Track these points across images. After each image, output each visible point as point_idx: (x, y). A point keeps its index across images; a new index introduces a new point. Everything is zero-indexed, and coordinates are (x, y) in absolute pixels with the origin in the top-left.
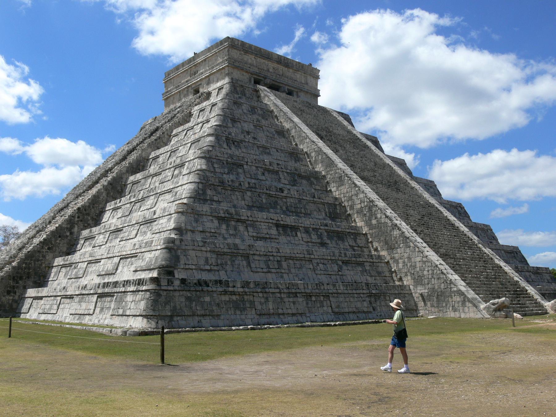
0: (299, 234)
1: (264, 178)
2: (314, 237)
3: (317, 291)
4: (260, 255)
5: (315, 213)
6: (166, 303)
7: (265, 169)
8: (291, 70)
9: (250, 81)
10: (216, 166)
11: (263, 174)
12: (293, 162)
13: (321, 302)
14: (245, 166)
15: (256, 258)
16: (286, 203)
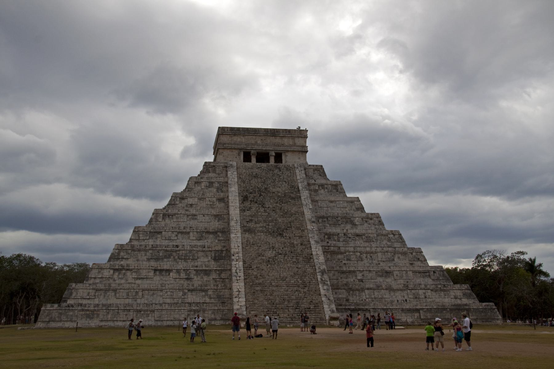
0: (171, 274)
1: (176, 238)
2: (183, 275)
3: (146, 308)
4: (124, 289)
5: (202, 258)
6: (47, 316)
7: (179, 233)
8: (278, 138)
10: (141, 236)
11: (177, 236)
12: (216, 221)
13: (148, 314)
14: (163, 233)
15: (122, 291)
16: (179, 254)
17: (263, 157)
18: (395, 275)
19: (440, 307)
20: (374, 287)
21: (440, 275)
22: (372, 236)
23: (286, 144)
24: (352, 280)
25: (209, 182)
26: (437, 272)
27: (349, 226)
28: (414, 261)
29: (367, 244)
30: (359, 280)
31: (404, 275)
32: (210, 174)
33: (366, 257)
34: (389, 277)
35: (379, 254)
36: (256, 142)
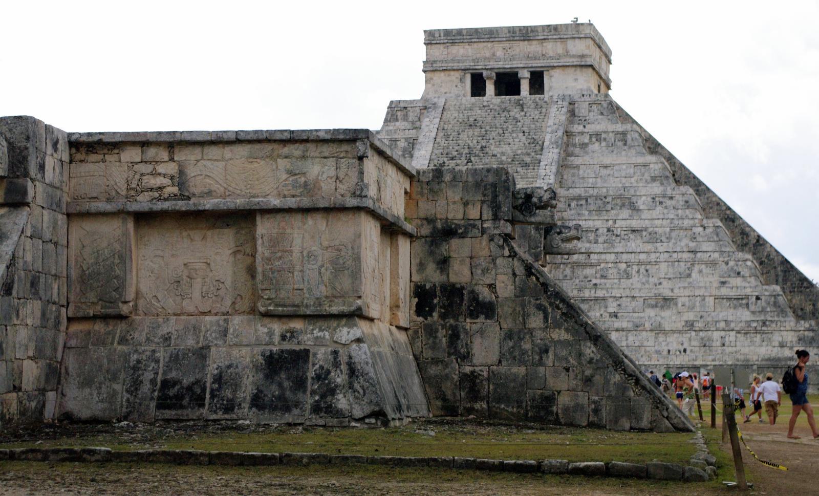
8: (534, 42)
9: (462, 80)
17: (508, 83)
18: (680, 305)
19: (739, 363)
20: (630, 325)
21: (769, 303)
22: (660, 230)
23: (551, 54)
24: (598, 314)
25: (391, 140)
26: (763, 298)
27: (625, 213)
28: (729, 276)
29: (649, 247)
30: (610, 314)
31: (698, 304)
32: (398, 124)
33: (638, 272)
34: (669, 307)
35: (663, 266)
36: (494, 55)
